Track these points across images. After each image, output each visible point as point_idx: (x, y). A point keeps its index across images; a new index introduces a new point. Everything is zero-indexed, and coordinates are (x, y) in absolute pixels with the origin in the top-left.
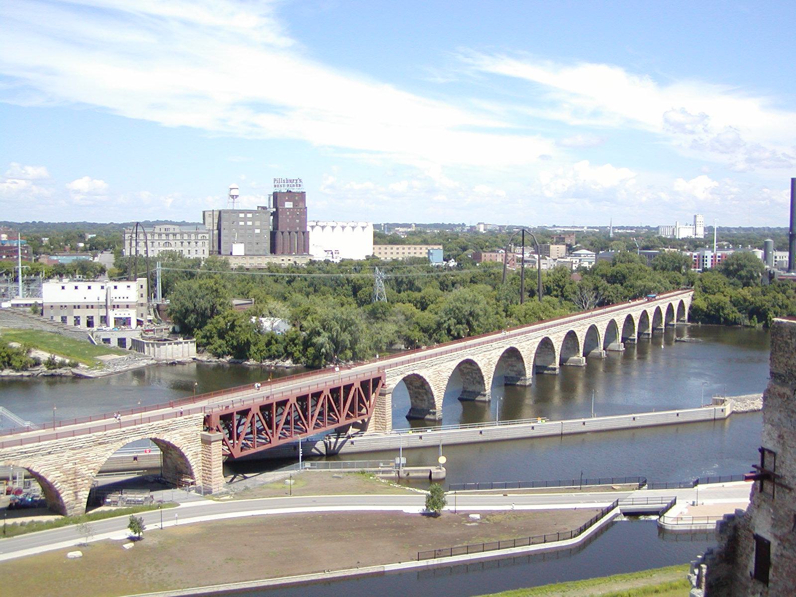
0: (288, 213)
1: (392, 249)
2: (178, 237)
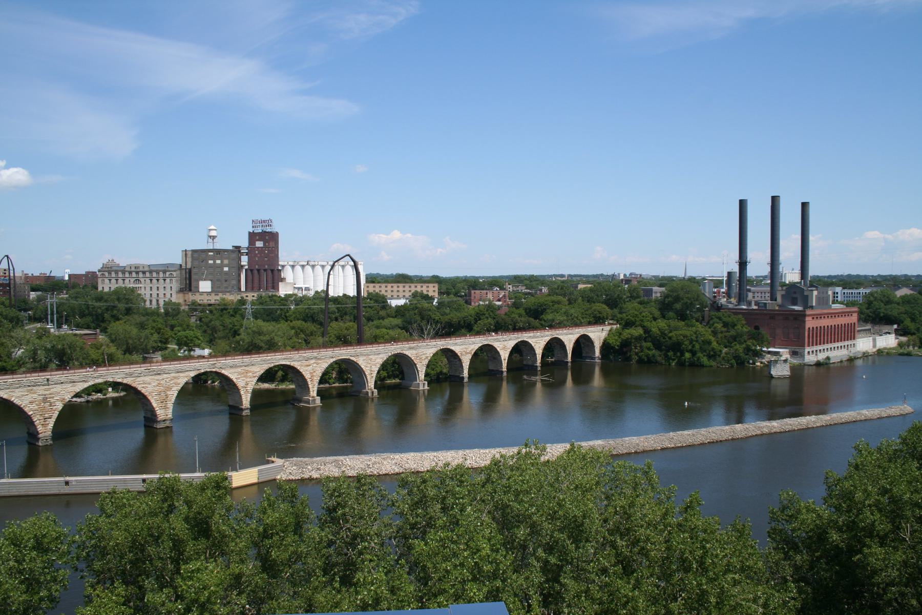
0: (257, 252)
1: (386, 287)
2: (148, 275)
